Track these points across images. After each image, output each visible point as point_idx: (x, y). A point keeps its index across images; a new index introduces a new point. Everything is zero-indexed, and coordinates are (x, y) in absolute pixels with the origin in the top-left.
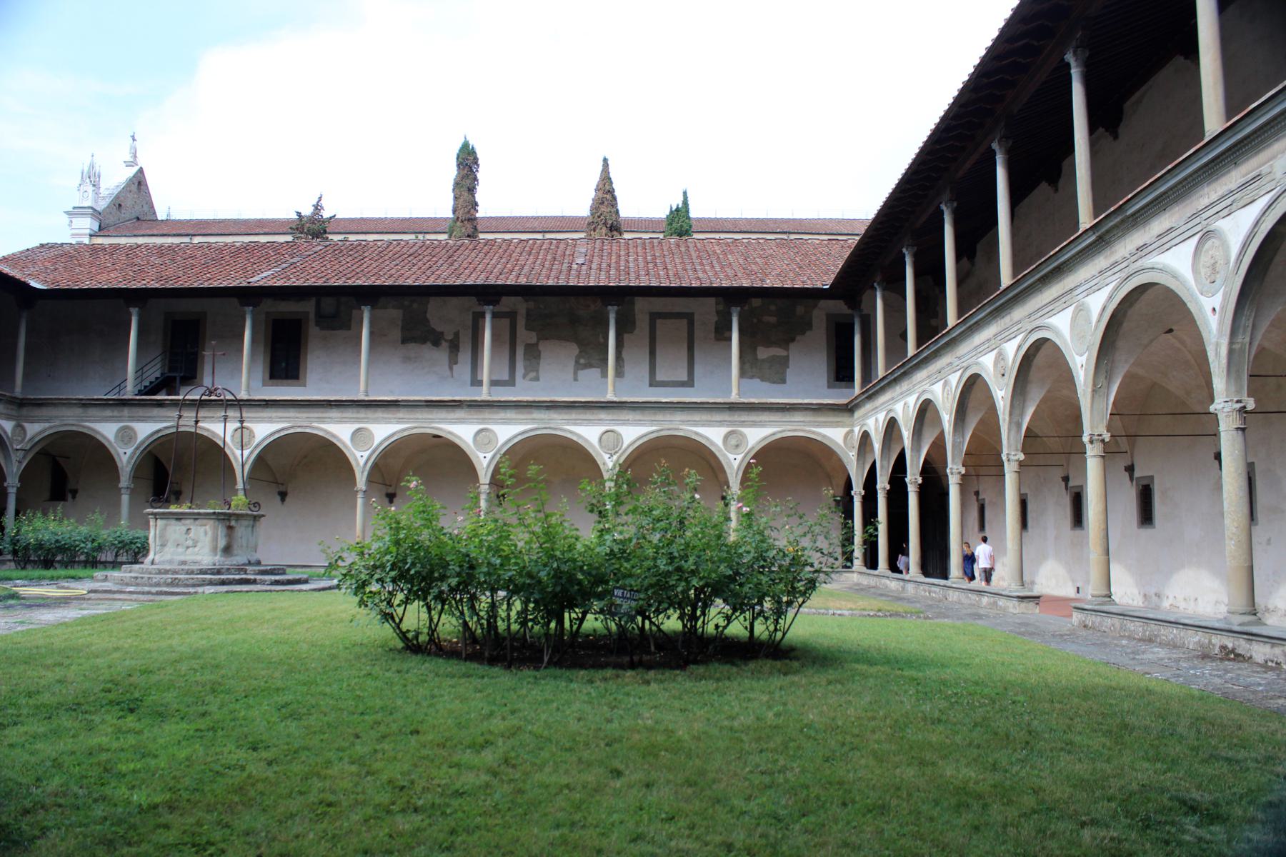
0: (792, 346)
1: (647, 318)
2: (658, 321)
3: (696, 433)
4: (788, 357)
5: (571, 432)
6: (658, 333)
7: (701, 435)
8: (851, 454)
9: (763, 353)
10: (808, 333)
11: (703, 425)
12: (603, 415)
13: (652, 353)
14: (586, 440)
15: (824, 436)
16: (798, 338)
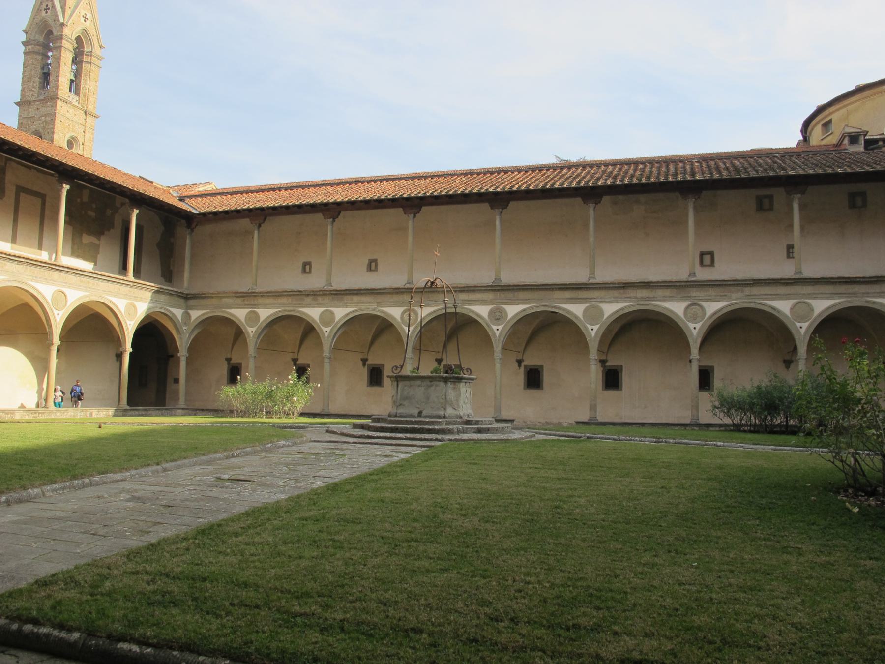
0: (102, 238)
1: (14, 188)
2: (22, 195)
3: (111, 302)
4: (98, 246)
5: (33, 287)
6: (21, 204)
7: (114, 304)
8: (184, 328)
9: (87, 239)
10: (112, 230)
11: (115, 296)
12: (55, 275)
13: (15, 221)
14: (44, 297)
15: (173, 314)
16: (106, 232)
